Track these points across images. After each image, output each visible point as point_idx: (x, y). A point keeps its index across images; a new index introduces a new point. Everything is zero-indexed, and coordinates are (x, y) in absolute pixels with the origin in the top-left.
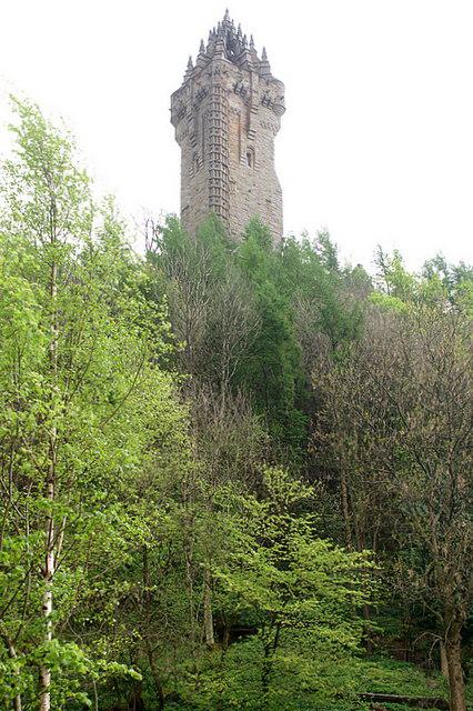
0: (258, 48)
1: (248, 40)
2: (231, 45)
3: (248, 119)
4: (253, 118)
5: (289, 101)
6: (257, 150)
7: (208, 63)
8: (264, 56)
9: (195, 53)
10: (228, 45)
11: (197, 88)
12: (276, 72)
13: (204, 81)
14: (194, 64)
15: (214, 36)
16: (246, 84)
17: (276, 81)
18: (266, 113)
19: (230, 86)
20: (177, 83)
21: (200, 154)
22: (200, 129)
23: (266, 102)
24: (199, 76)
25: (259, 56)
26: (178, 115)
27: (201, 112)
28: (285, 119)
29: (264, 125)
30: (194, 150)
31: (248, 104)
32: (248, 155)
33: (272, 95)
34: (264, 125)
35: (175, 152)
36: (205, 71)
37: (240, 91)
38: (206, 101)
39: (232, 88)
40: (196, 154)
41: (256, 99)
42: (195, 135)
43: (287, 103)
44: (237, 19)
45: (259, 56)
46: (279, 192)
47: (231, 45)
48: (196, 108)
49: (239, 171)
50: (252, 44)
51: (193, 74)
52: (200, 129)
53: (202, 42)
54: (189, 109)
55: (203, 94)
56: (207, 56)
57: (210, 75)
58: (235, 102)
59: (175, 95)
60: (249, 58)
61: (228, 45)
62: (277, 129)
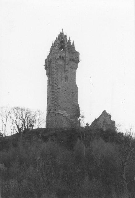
0: (72, 42)
2: (62, 42)
3: (65, 66)
4: (66, 66)
6: (68, 76)
8: (73, 44)
11: (50, 58)
12: (77, 49)
15: (57, 39)
18: (72, 63)
23: (71, 60)
25: (72, 45)
28: (79, 65)
29: (71, 68)
31: (65, 61)
32: (66, 78)
33: (74, 57)
34: (71, 68)
35: (46, 78)
37: (62, 58)
39: (59, 57)
41: (67, 60)
46: (76, 89)
47: (62, 42)
50: (70, 40)
53: (53, 42)
58: (60, 62)
59: (46, 60)
62: (77, 67)
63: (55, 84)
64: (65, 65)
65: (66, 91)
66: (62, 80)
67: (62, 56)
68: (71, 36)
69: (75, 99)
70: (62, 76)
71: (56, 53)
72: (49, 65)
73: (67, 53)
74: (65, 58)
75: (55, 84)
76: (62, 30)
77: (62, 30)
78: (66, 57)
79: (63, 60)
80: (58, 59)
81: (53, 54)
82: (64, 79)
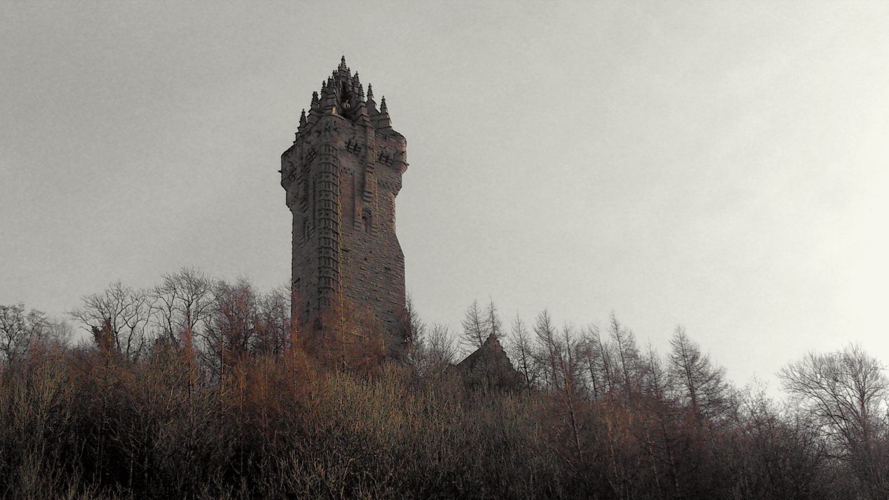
1: (365, 90)
2: (346, 96)
3: (364, 179)
5: (411, 154)
9: (308, 108)
11: (306, 147)
12: (395, 126)
13: (313, 138)
15: (327, 89)
17: (398, 137)
18: (385, 173)
19: (341, 144)
20: (289, 141)
21: (311, 220)
22: (311, 191)
23: (384, 159)
24: (309, 133)
25: (378, 108)
26: (288, 177)
27: (312, 174)
30: (304, 215)
31: (363, 161)
33: (390, 151)
35: (286, 218)
36: (315, 128)
40: (306, 220)
41: (372, 157)
42: (305, 199)
43: (409, 158)
44: (353, 68)
45: (378, 108)
46: (399, 258)
48: (306, 169)
52: (311, 191)
54: (299, 170)
55: (313, 153)
57: (320, 132)
58: (347, 162)
59: (285, 155)
60: (364, 111)
62: (399, 186)
63: (334, 232)
64: (363, 176)
65: (365, 262)
66: (354, 222)
67: (353, 141)
68: (378, 81)
69: (395, 291)
70: (353, 210)
71: (335, 130)
73: (371, 133)
74: (363, 150)
75: (334, 232)
76: (343, 59)
77: (343, 59)
78: (366, 146)
79: (357, 155)
80: (342, 150)
81: (323, 134)
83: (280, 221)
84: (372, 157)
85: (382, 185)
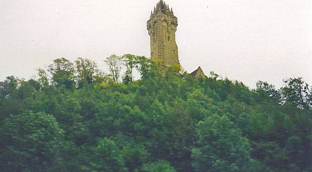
7: (157, 13)
8: (172, 10)
9: (153, 10)
10: (162, 8)
14: (153, 13)
16: (167, 19)
17: (175, 17)
18: (173, 26)
23: (173, 23)
26: (149, 27)
31: (168, 24)
33: (174, 21)
37: (165, 21)
38: (156, 24)
40: (154, 38)
42: (154, 33)
46: (177, 48)
49: (166, 43)
51: (153, 16)
54: (152, 26)
55: (155, 22)
56: (156, 11)
61: (162, 8)
72: (152, 26)
82: (167, 38)
83: (147, 38)
84: (170, 23)
85: (172, 30)
